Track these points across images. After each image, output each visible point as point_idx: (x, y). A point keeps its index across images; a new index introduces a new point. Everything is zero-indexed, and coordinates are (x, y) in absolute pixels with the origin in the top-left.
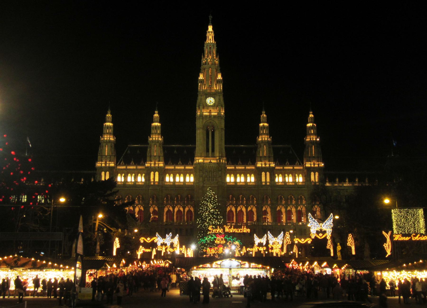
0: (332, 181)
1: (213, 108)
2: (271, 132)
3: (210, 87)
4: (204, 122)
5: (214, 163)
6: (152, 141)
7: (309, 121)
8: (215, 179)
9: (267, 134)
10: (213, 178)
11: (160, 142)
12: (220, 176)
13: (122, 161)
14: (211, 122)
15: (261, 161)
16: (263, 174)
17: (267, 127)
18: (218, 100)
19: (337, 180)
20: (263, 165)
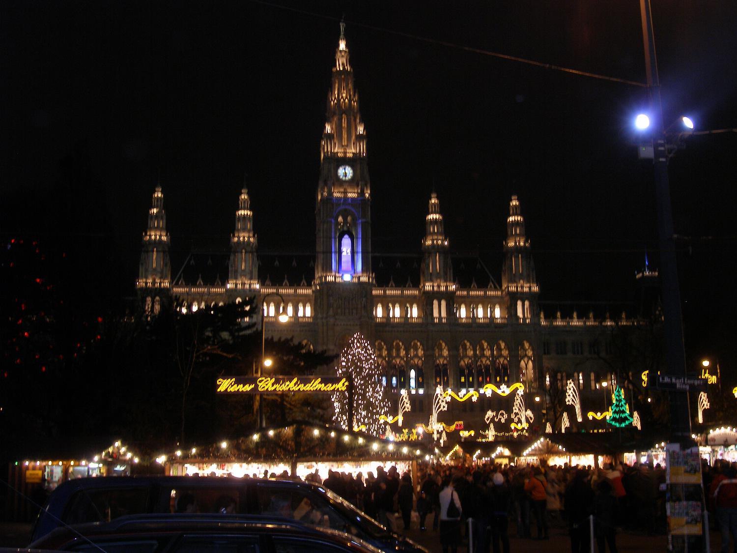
0: (551, 316)
2: (447, 227)
3: (345, 147)
6: (239, 242)
7: (511, 212)
8: (354, 311)
9: (441, 234)
10: (352, 309)
11: (253, 245)
12: (364, 306)
13: (182, 279)
14: (345, 210)
15: (431, 280)
16: (435, 303)
17: (441, 222)
18: (358, 172)
19: (559, 314)
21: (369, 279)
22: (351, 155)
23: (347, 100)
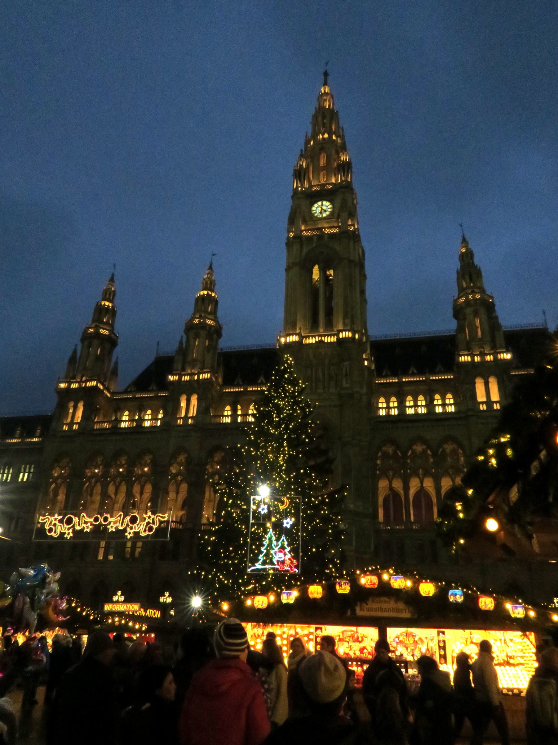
1: (328, 223)
4: (305, 250)
5: (331, 342)
12: (346, 375)
20: (476, 358)
21: (354, 335)
22: (330, 187)
23: (326, 136)
